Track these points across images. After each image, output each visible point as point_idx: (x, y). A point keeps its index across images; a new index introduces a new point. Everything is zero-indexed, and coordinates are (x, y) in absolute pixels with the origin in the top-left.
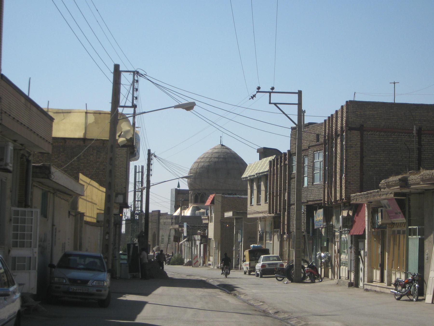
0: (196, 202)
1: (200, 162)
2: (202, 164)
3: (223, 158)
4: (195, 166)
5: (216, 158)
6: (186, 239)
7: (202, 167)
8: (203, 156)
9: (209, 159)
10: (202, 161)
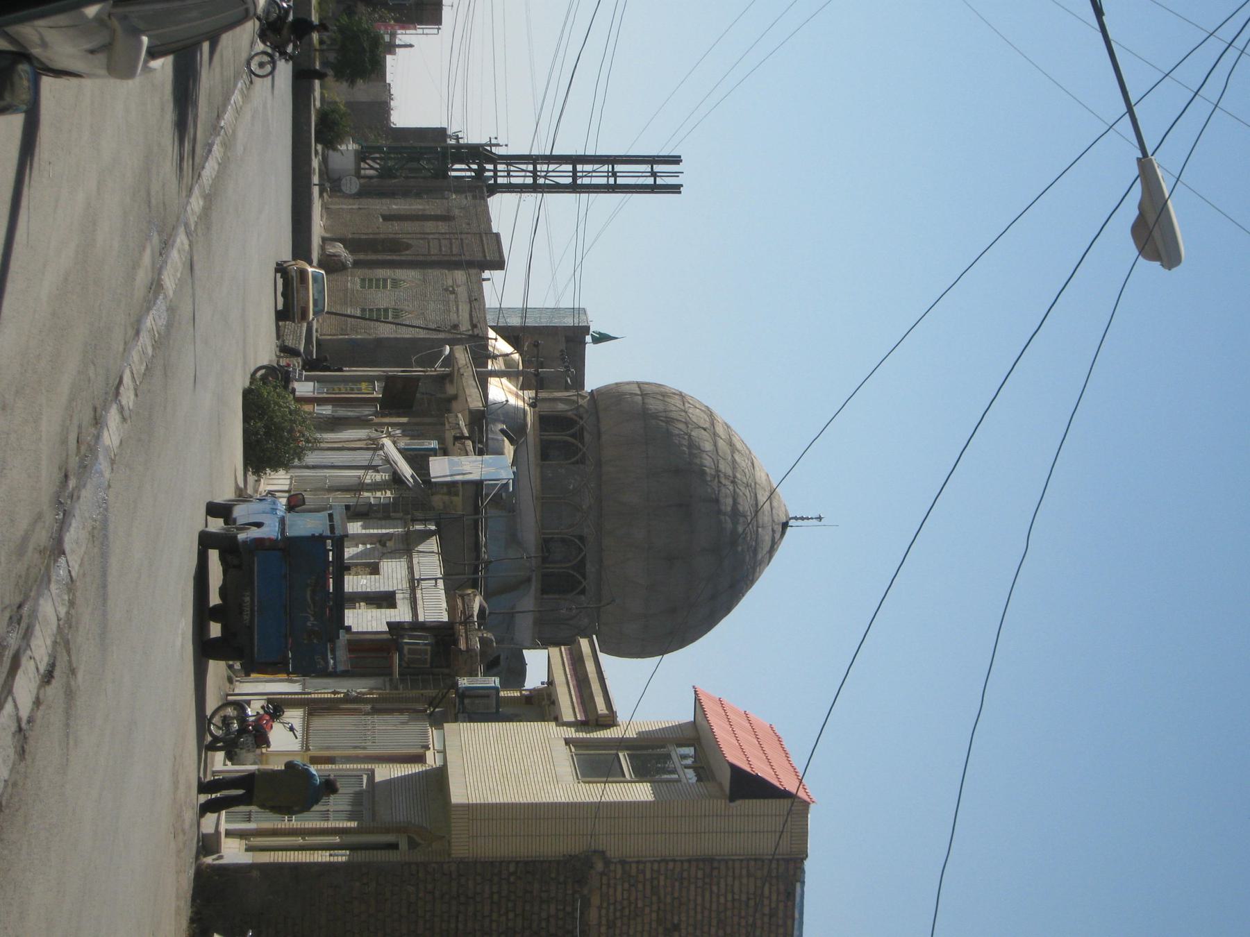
0: (545, 421)
1: (715, 434)
2: (708, 446)
3: (734, 531)
4: (698, 417)
5: (735, 503)
6: (406, 470)
7: (693, 446)
8: (739, 445)
9: (730, 472)
10: (721, 443)
